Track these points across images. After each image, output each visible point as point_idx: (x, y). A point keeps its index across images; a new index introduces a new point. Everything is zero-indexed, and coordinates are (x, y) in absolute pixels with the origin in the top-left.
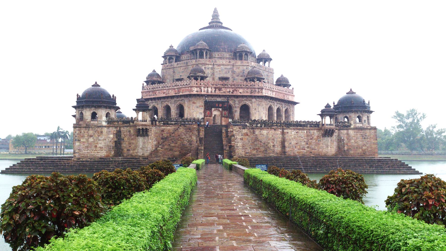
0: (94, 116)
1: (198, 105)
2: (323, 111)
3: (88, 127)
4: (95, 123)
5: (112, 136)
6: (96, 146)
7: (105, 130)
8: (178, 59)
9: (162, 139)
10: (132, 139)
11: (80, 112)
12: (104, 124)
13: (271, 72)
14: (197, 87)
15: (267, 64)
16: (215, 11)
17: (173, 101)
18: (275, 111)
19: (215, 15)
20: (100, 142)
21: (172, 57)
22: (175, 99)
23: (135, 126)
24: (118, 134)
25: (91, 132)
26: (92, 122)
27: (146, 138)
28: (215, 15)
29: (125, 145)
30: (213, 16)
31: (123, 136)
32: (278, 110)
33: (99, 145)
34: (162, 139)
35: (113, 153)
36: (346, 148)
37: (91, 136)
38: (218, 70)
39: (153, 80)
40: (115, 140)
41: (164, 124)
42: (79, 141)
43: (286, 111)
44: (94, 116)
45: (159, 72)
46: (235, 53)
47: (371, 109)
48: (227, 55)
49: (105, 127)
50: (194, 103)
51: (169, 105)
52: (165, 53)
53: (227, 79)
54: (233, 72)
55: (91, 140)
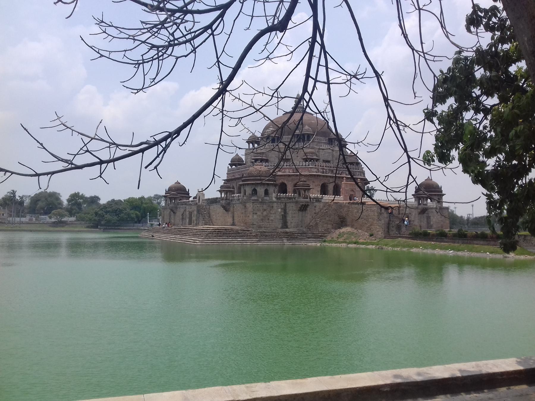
0: (266, 193)
1: (316, 184)
3: (263, 202)
4: (268, 198)
5: (280, 210)
6: (268, 219)
7: (275, 205)
9: (315, 213)
10: (295, 213)
11: (253, 188)
12: (274, 199)
14: (315, 168)
17: (290, 178)
20: (272, 215)
22: (293, 177)
23: (297, 202)
24: (285, 210)
25: (265, 207)
26: (265, 198)
27: (304, 212)
29: (289, 218)
31: (288, 210)
33: (271, 218)
34: (315, 213)
35: (280, 226)
36: (432, 223)
37: (265, 210)
38: (322, 153)
40: (283, 213)
41: (316, 201)
42: (256, 214)
44: (266, 193)
46: (329, 139)
47: (443, 193)
48: (324, 140)
49: (275, 202)
50: (313, 182)
51: (286, 182)
53: (328, 162)
54: (333, 156)
55: (265, 213)
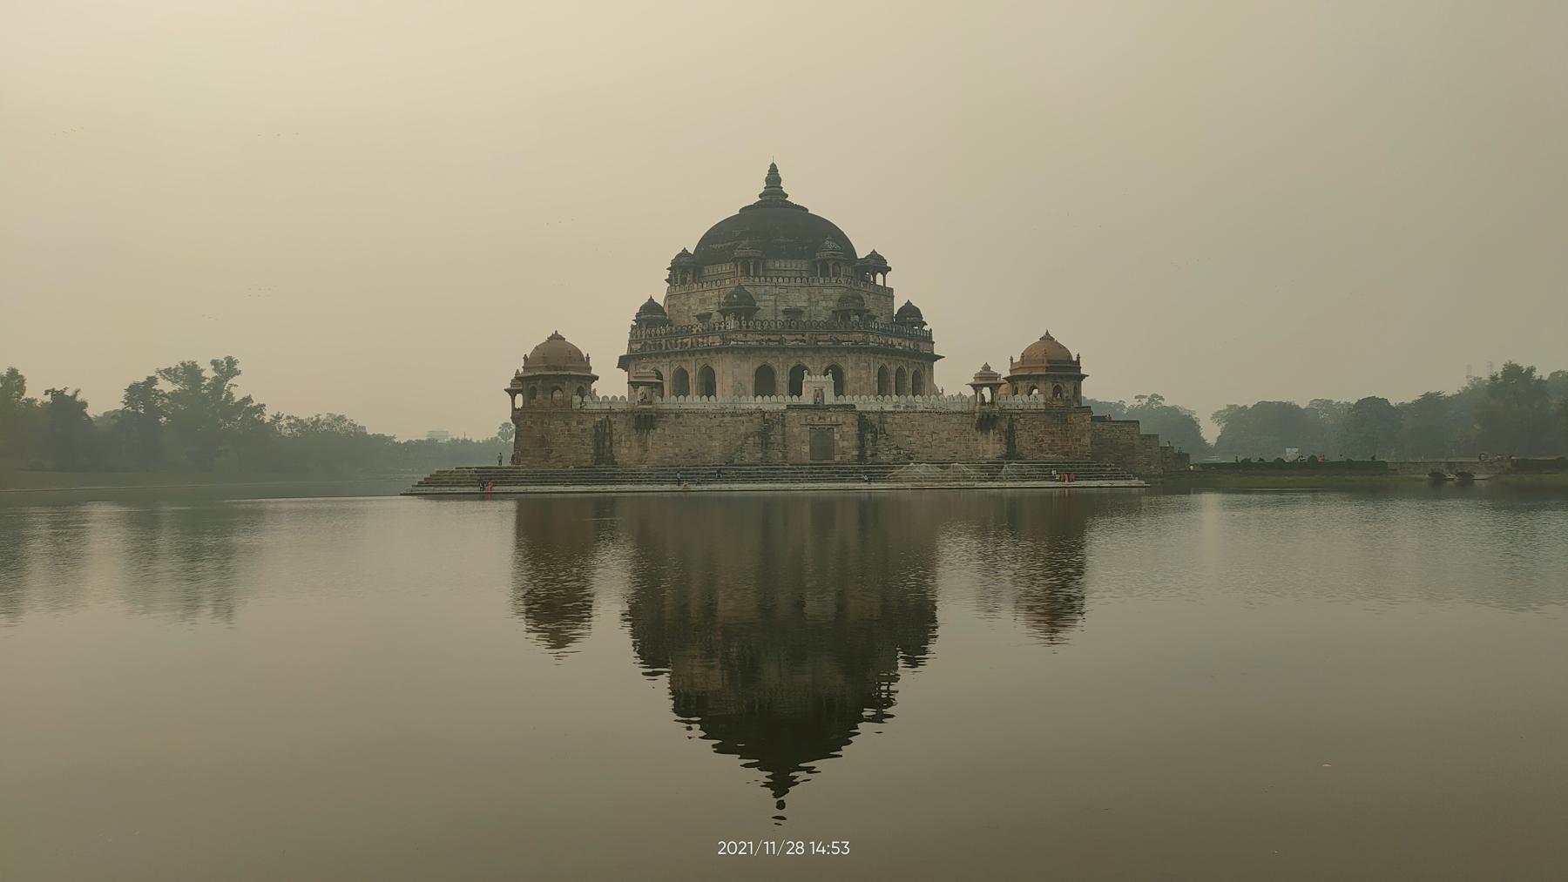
2: (979, 377)
8: (698, 277)
13: (889, 294)
15: (879, 277)
16: (773, 169)
18: (893, 378)
19: (773, 177)
21: (685, 269)
28: (773, 177)
30: (767, 180)
32: (900, 374)
39: (649, 315)
43: (917, 377)
45: (660, 301)
52: (673, 262)
53: (799, 312)
